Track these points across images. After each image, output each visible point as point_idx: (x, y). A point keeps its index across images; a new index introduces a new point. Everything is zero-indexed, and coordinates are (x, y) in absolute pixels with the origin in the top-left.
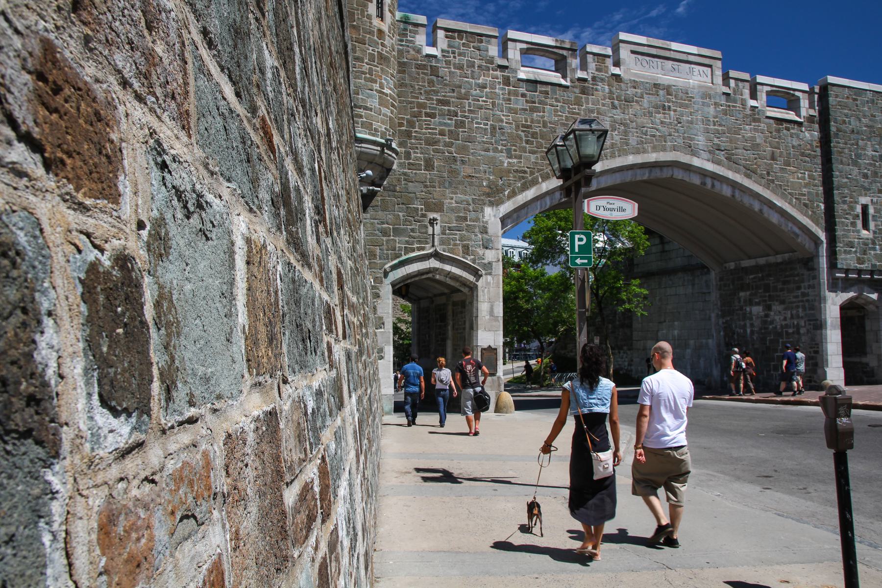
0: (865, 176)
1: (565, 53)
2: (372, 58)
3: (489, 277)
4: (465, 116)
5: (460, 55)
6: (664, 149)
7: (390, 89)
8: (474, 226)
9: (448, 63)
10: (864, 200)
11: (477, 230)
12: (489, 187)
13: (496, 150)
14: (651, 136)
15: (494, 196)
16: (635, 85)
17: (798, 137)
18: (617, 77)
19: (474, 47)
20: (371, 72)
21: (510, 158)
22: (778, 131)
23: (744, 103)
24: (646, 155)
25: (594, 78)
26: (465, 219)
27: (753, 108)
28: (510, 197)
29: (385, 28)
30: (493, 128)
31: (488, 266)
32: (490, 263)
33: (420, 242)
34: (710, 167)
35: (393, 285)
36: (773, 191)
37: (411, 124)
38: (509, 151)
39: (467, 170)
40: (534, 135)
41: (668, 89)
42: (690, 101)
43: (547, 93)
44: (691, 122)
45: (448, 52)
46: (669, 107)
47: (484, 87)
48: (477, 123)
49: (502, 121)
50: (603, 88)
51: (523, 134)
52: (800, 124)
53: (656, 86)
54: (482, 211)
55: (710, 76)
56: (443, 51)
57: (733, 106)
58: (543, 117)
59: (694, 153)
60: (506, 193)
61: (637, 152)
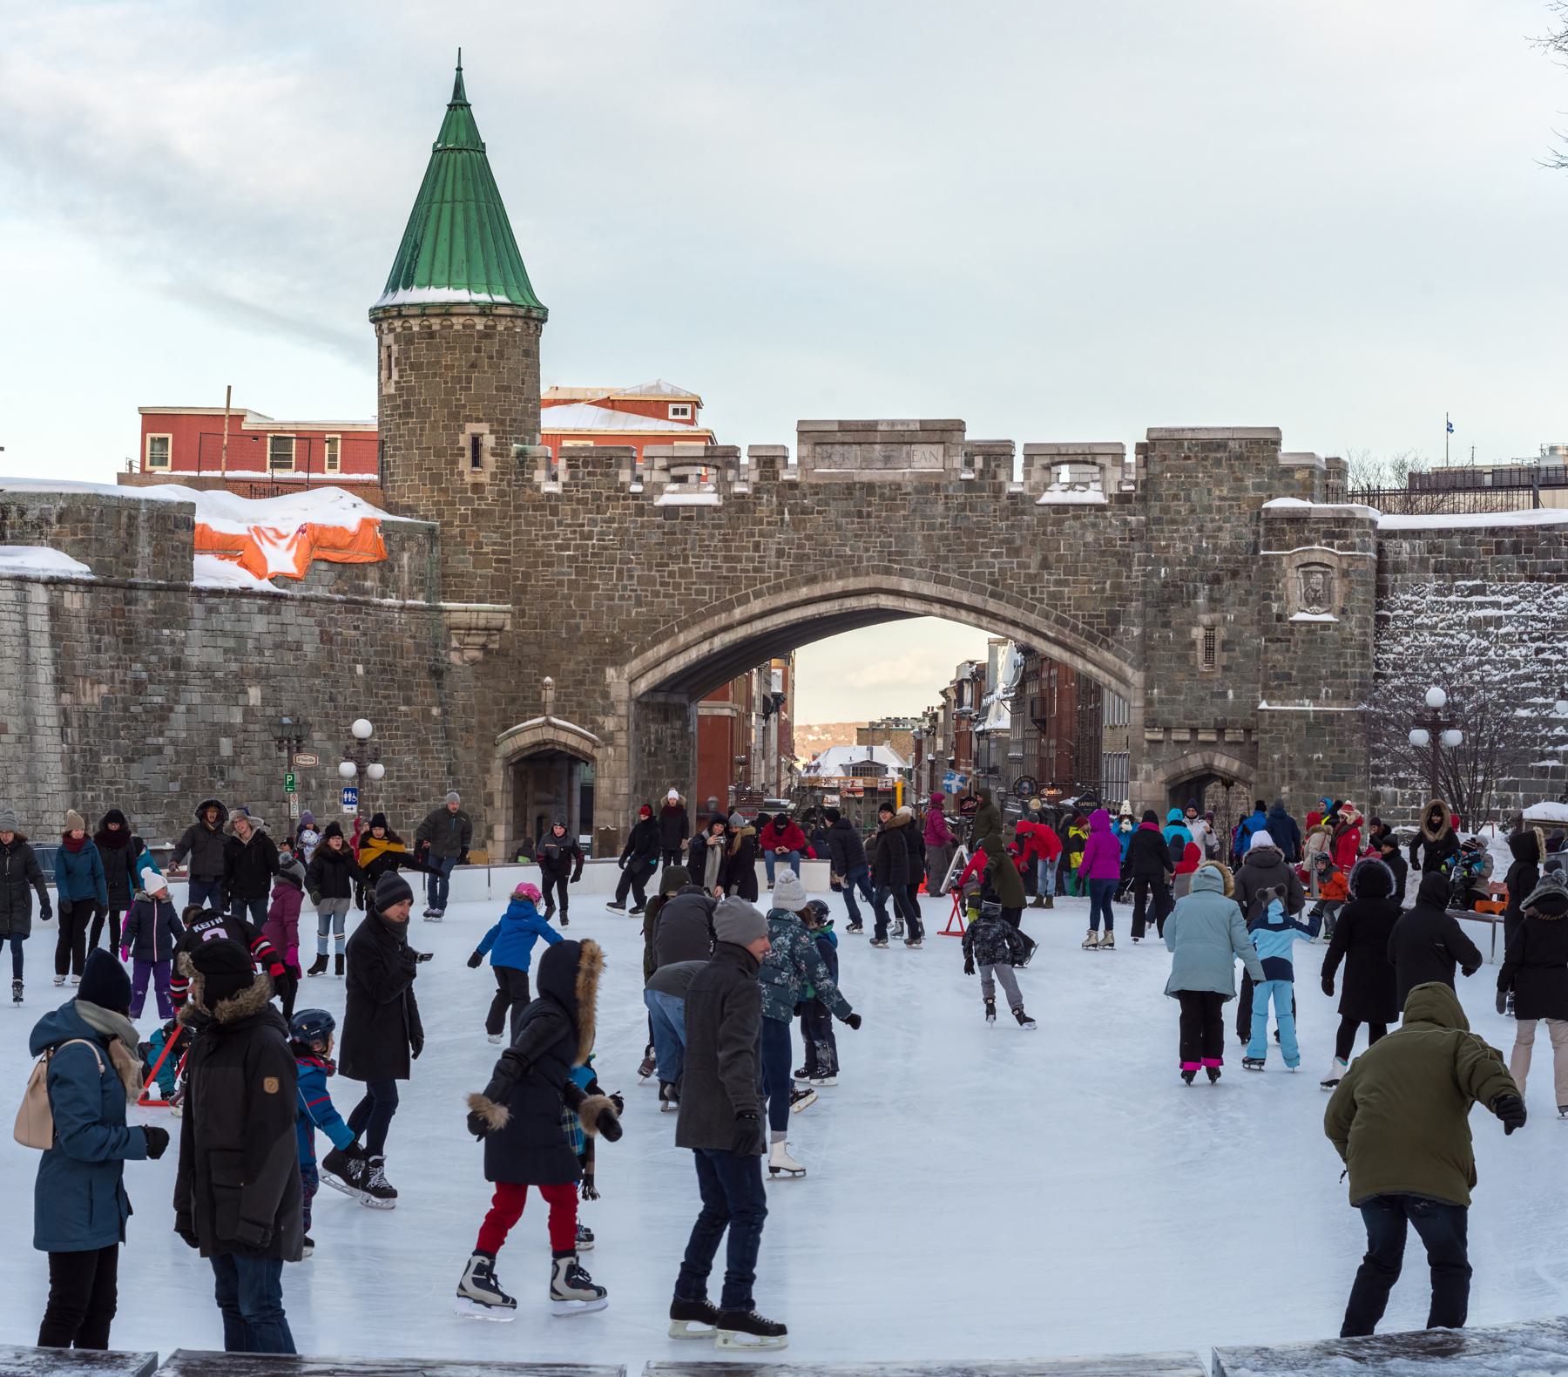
1: (719, 462)
2: (464, 518)
3: (610, 750)
4: (588, 562)
5: (585, 486)
6: (857, 573)
7: (495, 544)
8: (594, 691)
9: (570, 499)
11: (597, 694)
12: (612, 643)
13: (622, 598)
14: (837, 556)
15: (616, 654)
16: (816, 489)
17: (1094, 525)
18: (793, 485)
19: (601, 475)
20: (462, 534)
21: (641, 606)
22: (1059, 523)
23: (998, 489)
24: (828, 584)
26: (581, 683)
27: (1013, 496)
28: (637, 655)
29: (485, 478)
30: (620, 572)
31: (609, 739)
32: (612, 733)
33: (532, 711)
37: (526, 576)
38: (638, 597)
39: (585, 625)
40: (671, 575)
41: (869, 487)
42: (905, 499)
43: (691, 518)
44: (905, 530)
45: (570, 485)
46: (869, 515)
47: (611, 520)
48: (601, 568)
49: (631, 561)
50: (768, 502)
51: (657, 574)
52: (1100, 508)
54: (603, 672)
55: (941, 458)
56: (564, 485)
57: (977, 497)
58: (685, 549)
60: (633, 649)
61: (812, 580)
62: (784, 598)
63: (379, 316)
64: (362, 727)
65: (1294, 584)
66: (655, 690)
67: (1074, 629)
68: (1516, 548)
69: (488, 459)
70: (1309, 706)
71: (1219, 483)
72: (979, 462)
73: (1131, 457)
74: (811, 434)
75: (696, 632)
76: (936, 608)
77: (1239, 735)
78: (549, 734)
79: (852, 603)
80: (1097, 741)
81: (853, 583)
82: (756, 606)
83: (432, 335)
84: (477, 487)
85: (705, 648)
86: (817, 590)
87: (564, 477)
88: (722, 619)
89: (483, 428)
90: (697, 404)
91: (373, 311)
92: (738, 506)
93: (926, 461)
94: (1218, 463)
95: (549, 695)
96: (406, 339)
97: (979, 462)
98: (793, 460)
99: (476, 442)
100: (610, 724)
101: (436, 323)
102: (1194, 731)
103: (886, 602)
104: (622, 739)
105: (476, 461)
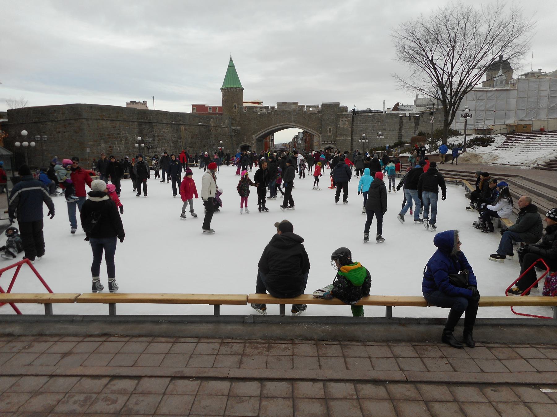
0: (331, 122)
6: (284, 122)
10: (330, 127)
15: (254, 133)
16: (280, 111)
18: (276, 111)
23: (303, 111)
25: (272, 112)
27: (305, 112)
29: (236, 110)
34: (294, 124)
35: (240, 147)
36: (308, 128)
41: (286, 111)
53: (284, 111)
59: (290, 122)
62: (275, 126)
63: (222, 89)
64: (221, 142)
65: (341, 123)
66: (259, 138)
67: (312, 129)
68: (370, 118)
69: (237, 108)
70: (343, 138)
71: (332, 109)
72: (300, 108)
73: (320, 107)
74: (279, 104)
75: (264, 130)
76: (295, 126)
77: (334, 143)
78: (245, 144)
79: (284, 126)
80: (313, 144)
81: (284, 124)
82: (272, 127)
83: (229, 92)
84: (235, 112)
85: (265, 132)
86: (279, 125)
87: (247, 110)
88: (267, 128)
89: (236, 104)
90: (262, 103)
91: (221, 89)
92: (269, 113)
93: (293, 107)
94: (331, 107)
95: (245, 139)
96: (225, 92)
97: (300, 108)
98: (276, 108)
99: (235, 106)
100: (253, 142)
101: (229, 90)
102: (328, 142)
103: (288, 126)
104: (255, 144)
105: (235, 108)
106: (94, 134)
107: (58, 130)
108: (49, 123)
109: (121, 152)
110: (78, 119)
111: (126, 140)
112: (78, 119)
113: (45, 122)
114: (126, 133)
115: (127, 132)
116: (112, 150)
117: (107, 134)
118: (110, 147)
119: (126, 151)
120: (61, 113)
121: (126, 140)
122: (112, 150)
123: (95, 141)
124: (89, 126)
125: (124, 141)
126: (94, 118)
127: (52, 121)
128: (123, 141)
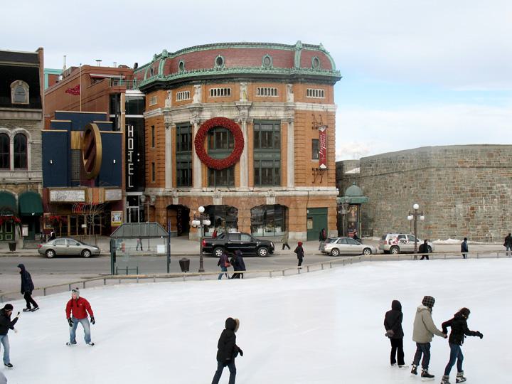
106: (447, 189)
107: (404, 184)
108: (396, 175)
109: (490, 217)
110: (427, 168)
111: (502, 197)
112: (427, 168)
113: (393, 173)
114: (503, 187)
115: (504, 185)
116: (475, 212)
117: (468, 188)
118: (472, 208)
119: (501, 214)
120: (409, 160)
121: (501, 197)
122: (475, 212)
123: (447, 200)
124: (441, 179)
125: (498, 198)
126: (449, 165)
127: (400, 172)
128: (496, 200)
